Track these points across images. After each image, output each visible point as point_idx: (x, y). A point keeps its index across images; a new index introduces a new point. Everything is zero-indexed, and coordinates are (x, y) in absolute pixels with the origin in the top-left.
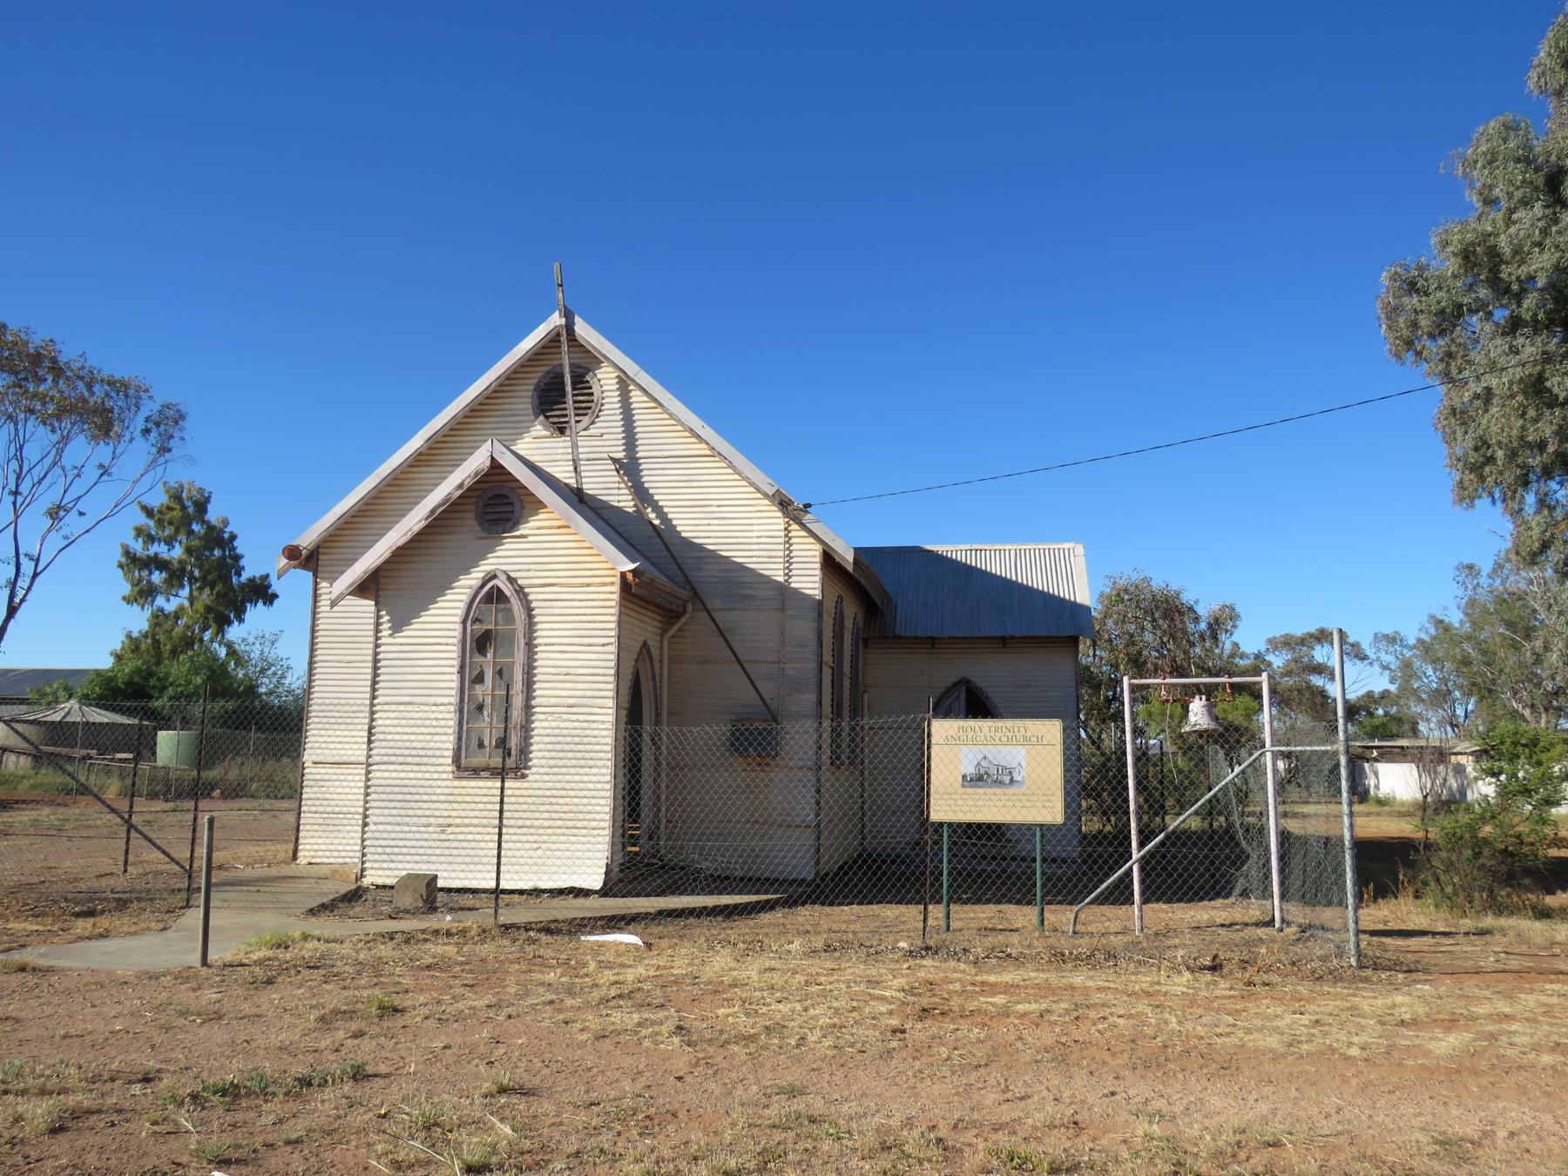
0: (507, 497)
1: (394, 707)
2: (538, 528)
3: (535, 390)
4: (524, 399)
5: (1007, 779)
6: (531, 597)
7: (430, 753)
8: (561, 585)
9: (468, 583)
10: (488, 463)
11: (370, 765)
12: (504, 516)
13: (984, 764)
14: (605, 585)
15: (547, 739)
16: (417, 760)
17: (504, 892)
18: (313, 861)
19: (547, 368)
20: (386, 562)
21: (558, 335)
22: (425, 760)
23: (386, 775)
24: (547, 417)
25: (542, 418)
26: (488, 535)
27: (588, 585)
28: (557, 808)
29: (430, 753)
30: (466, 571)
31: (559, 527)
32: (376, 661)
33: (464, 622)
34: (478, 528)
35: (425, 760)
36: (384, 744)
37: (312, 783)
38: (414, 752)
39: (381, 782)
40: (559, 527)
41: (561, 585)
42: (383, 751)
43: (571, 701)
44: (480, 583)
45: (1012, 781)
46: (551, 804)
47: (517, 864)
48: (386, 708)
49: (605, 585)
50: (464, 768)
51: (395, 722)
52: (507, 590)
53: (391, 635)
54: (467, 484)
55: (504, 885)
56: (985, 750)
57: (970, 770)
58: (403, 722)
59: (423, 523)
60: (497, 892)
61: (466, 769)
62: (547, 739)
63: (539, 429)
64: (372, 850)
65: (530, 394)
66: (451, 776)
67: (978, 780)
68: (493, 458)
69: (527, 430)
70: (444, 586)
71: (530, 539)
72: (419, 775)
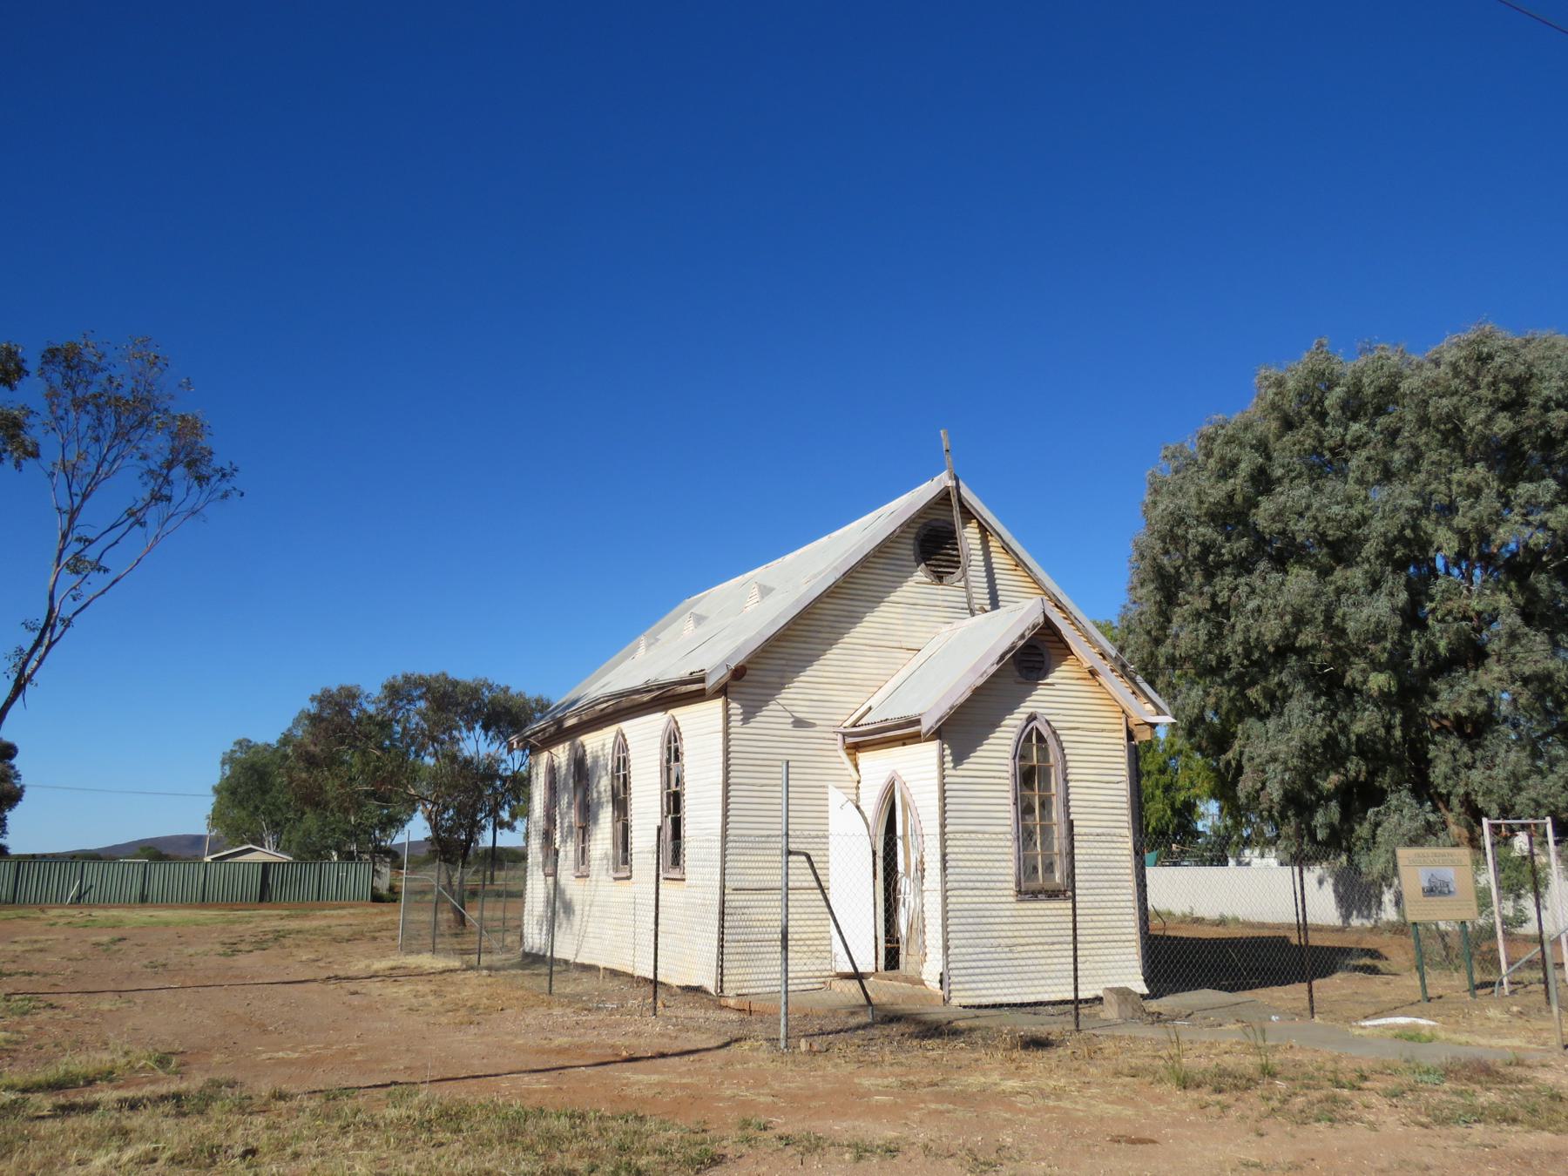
1: (966, 836)
2: (1063, 678)
3: (916, 539)
4: (908, 550)
5: (1446, 890)
6: (1062, 738)
7: (994, 878)
8: (1083, 729)
9: (1013, 723)
10: (1041, 620)
11: (947, 891)
12: (1037, 665)
14: (1115, 731)
15: (1086, 865)
17: (1080, 1001)
18: (739, 992)
20: (968, 700)
21: (948, 493)
22: (992, 885)
25: (923, 565)
26: (1024, 681)
27: (1103, 730)
29: (994, 878)
31: (1078, 679)
33: (1014, 758)
34: (1017, 674)
35: (992, 885)
36: (957, 870)
37: (732, 911)
38: (981, 878)
41: (1083, 729)
42: (959, 878)
43: (1099, 831)
44: (1025, 724)
45: (1449, 892)
49: (1115, 731)
50: (1027, 893)
51: (963, 850)
52: (1045, 732)
53: (954, 768)
54: (1028, 635)
55: (1081, 996)
56: (1434, 869)
57: (1426, 885)
58: (971, 850)
59: (996, 667)
60: (1077, 1002)
62: (1086, 865)
63: (921, 574)
67: (1431, 891)
68: (1046, 617)
70: (994, 725)
71: (1057, 687)
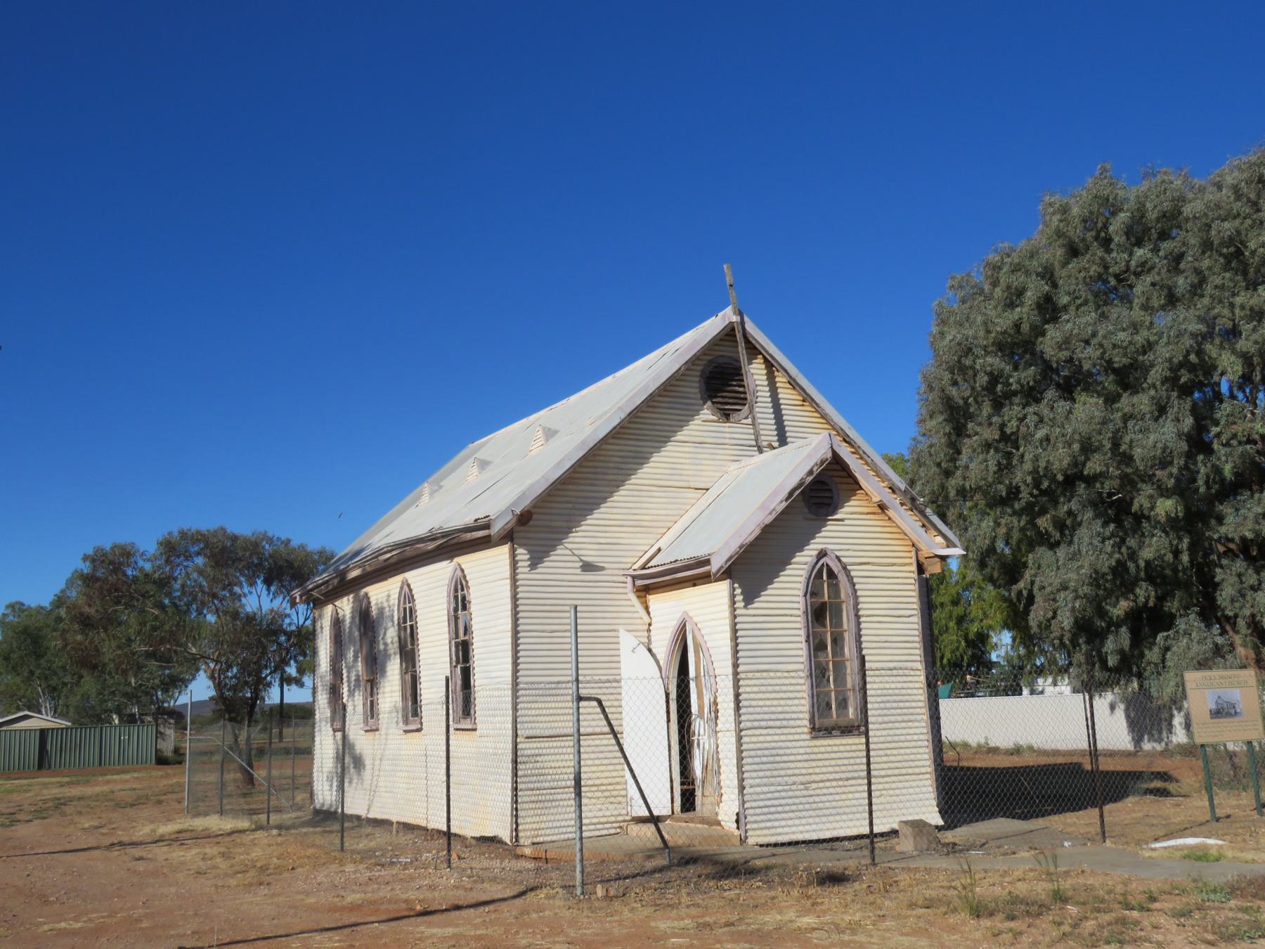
0: (828, 485)
1: (758, 675)
2: (852, 514)
3: (701, 376)
4: (694, 388)
5: (1233, 711)
6: (853, 574)
7: (788, 716)
8: (873, 564)
9: (804, 560)
10: (829, 455)
11: (741, 731)
12: (826, 501)
13: (1220, 701)
14: (905, 565)
15: (879, 699)
16: (778, 723)
17: (876, 835)
18: (535, 840)
19: (710, 358)
20: (757, 539)
21: (733, 329)
22: (785, 723)
23: (754, 739)
24: (713, 403)
25: (709, 403)
26: (813, 517)
27: (893, 565)
28: (892, 758)
29: (788, 716)
30: (800, 548)
31: (868, 514)
32: (735, 631)
33: (805, 595)
34: (806, 510)
35: (785, 723)
36: (751, 710)
37: (524, 759)
38: (773, 717)
39: (752, 746)
40: (868, 514)
41: (873, 564)
42: (752, 717)
43: (891, 665)
44: (815, 561)
45: (1236, 713)
46: (886, 755)
47: (885, 809)
48: (750, 675)
49: (905, 565)
50: (821, 728)
51: (755, 689)
52: (836, 568)
53: (745, 607)
54: (816, 471)
55: (876, 830)
56: (1220, 692)
57: (1213, 707)
58: (763, 689)
59: (784, 504)
60: (872, 836)
61: (820, 730)
62: (879, 699)
63: (707, 413)
64: (751, 811)
65: (698, 379)
66: (808, 737)
67: (1218, 713)
68: (834, 453)
69: (697, 412)
70: (785, 562)
71: (847, 522)
72: (783, 738)
